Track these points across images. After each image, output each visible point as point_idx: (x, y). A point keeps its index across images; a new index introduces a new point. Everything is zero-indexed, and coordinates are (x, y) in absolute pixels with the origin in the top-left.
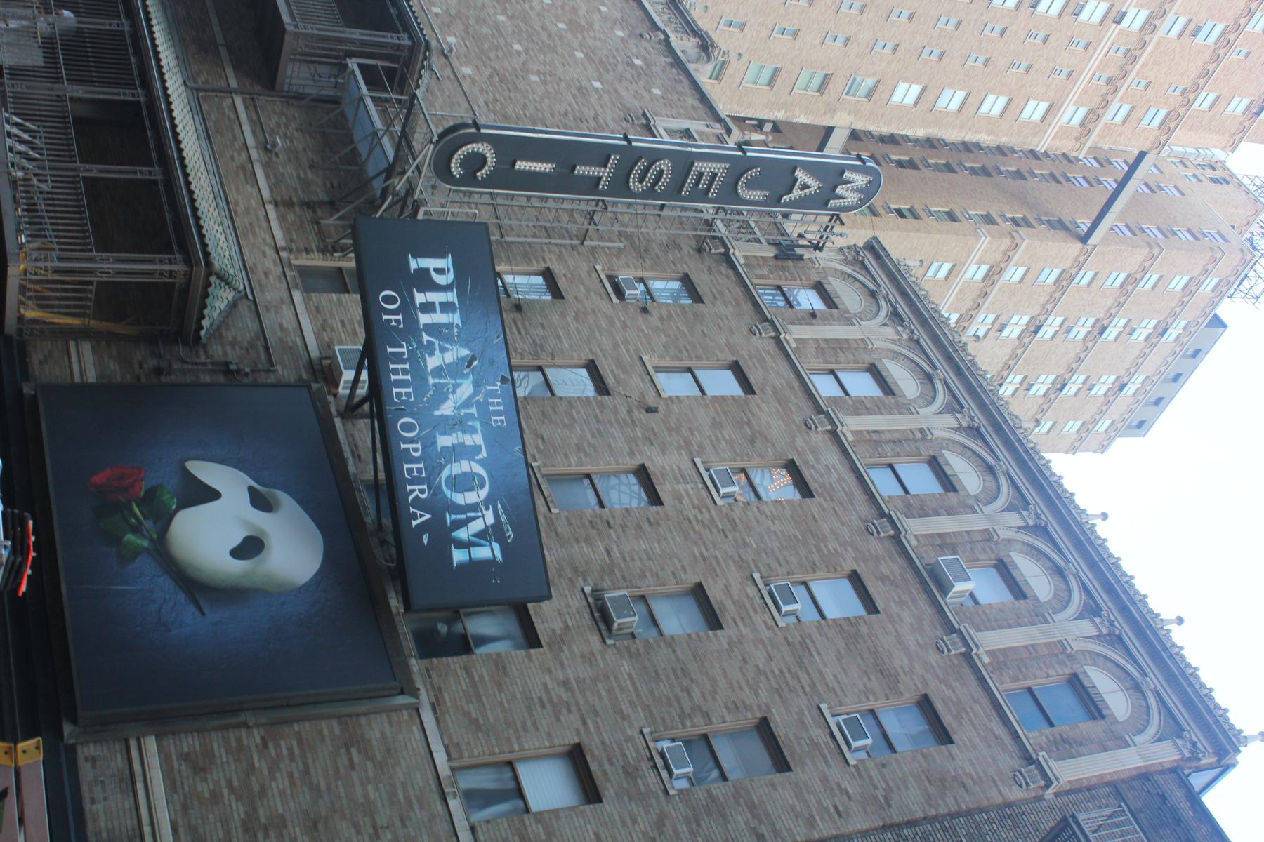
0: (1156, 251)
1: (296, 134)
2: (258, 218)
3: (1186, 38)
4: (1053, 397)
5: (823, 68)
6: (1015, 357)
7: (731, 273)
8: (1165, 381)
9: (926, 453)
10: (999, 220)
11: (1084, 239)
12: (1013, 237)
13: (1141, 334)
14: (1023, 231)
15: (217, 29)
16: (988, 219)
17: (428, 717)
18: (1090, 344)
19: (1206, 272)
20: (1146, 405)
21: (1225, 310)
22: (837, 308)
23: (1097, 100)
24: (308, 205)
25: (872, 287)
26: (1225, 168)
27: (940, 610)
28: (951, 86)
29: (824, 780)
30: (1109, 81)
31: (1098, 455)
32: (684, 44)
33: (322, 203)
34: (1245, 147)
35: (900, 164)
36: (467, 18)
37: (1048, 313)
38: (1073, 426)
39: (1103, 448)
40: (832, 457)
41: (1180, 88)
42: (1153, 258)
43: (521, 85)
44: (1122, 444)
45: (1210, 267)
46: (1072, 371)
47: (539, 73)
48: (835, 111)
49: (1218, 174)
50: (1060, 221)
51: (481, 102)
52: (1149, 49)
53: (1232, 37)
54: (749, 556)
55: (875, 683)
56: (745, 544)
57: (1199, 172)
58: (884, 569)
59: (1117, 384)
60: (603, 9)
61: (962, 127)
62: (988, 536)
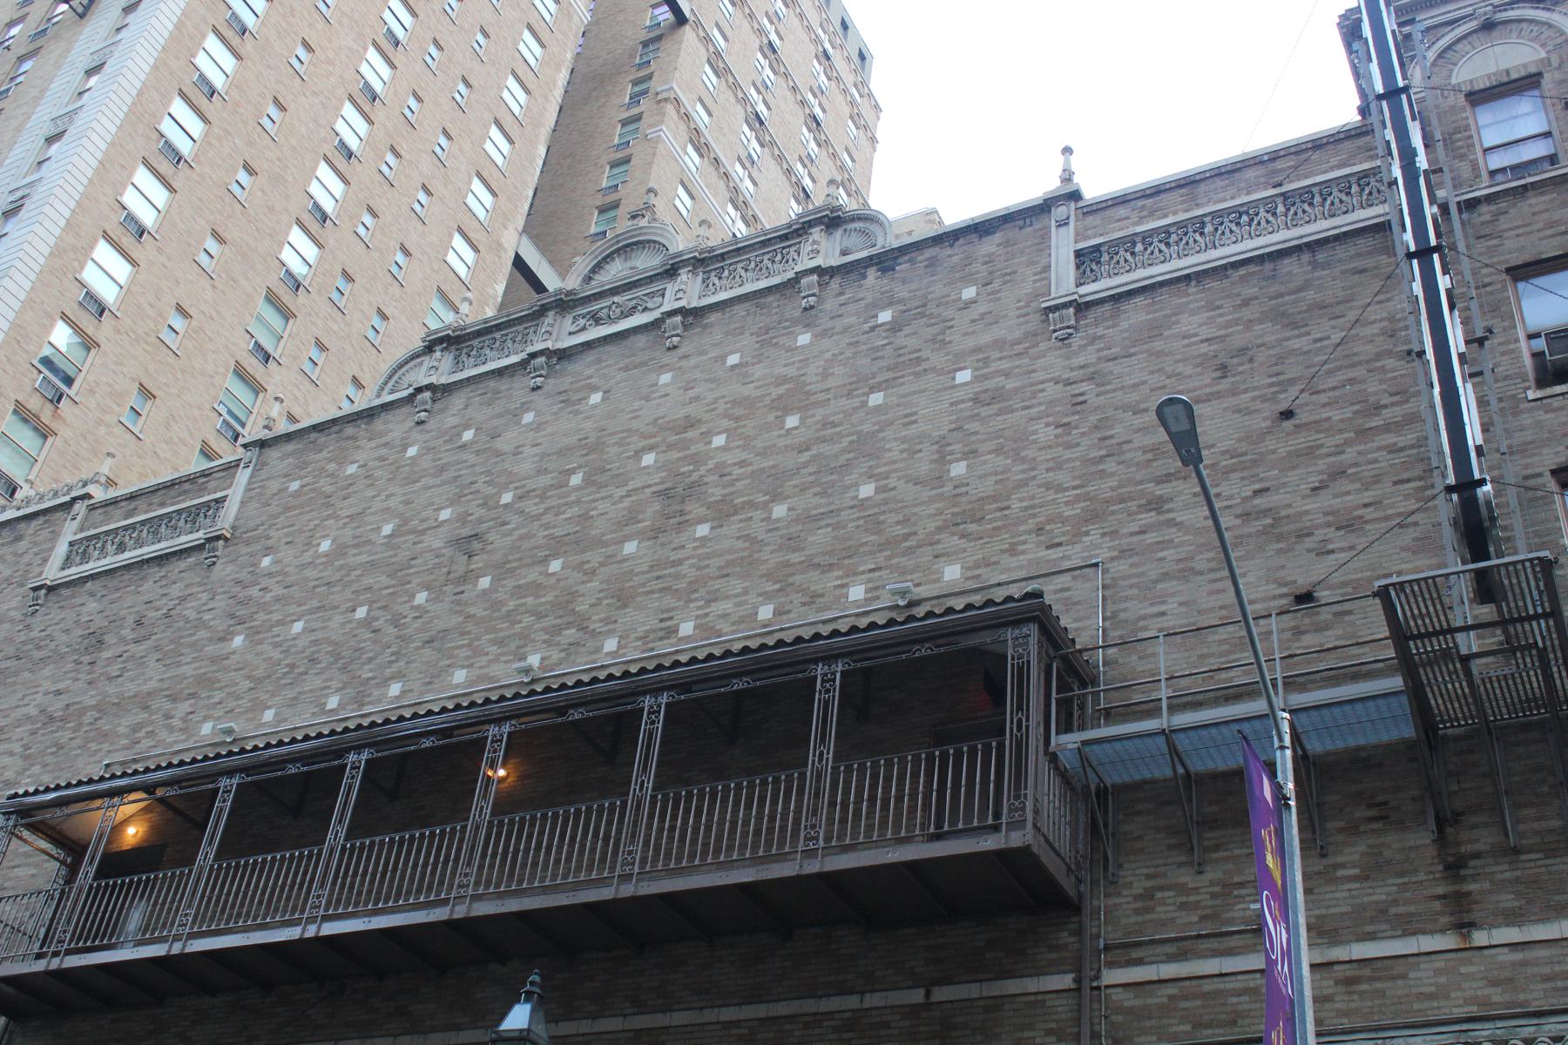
1: (1211, 874)
2: (1525, 963)
5: (451, 236)
6: (780, 158)
7: (1484, 208)
10: (635, 111)
11: (681, 19)
12: (666, 100)
14: (656, 85)
15: (873, 1000)
18: (782, 69)
22: (1540, 74)
24: (1455, 867)
25: (1473, 25)
28: (500, 89)
32: (826, 250)
33: (1441, 839)
36: (788, 564)
43: (988, 487)
44: (879, 82)
47: (943, 460)
48: (500, 244)
50: (645, 44)
51: (1043, 553)
59: (823, 60)
60: (733, 359)
61: (546, 99)
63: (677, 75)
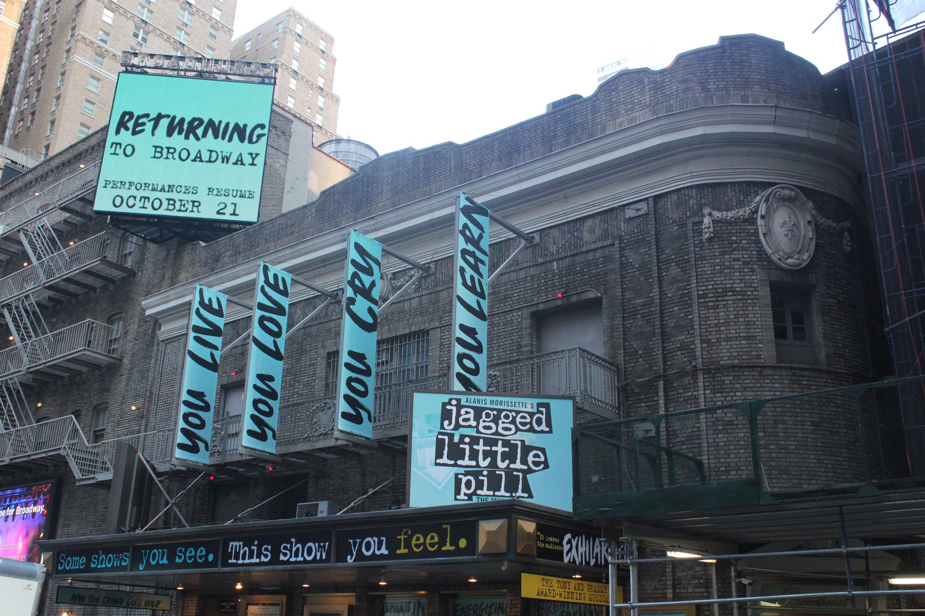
4: (194, 9)
16: (68, 51)
63: (83, 26)
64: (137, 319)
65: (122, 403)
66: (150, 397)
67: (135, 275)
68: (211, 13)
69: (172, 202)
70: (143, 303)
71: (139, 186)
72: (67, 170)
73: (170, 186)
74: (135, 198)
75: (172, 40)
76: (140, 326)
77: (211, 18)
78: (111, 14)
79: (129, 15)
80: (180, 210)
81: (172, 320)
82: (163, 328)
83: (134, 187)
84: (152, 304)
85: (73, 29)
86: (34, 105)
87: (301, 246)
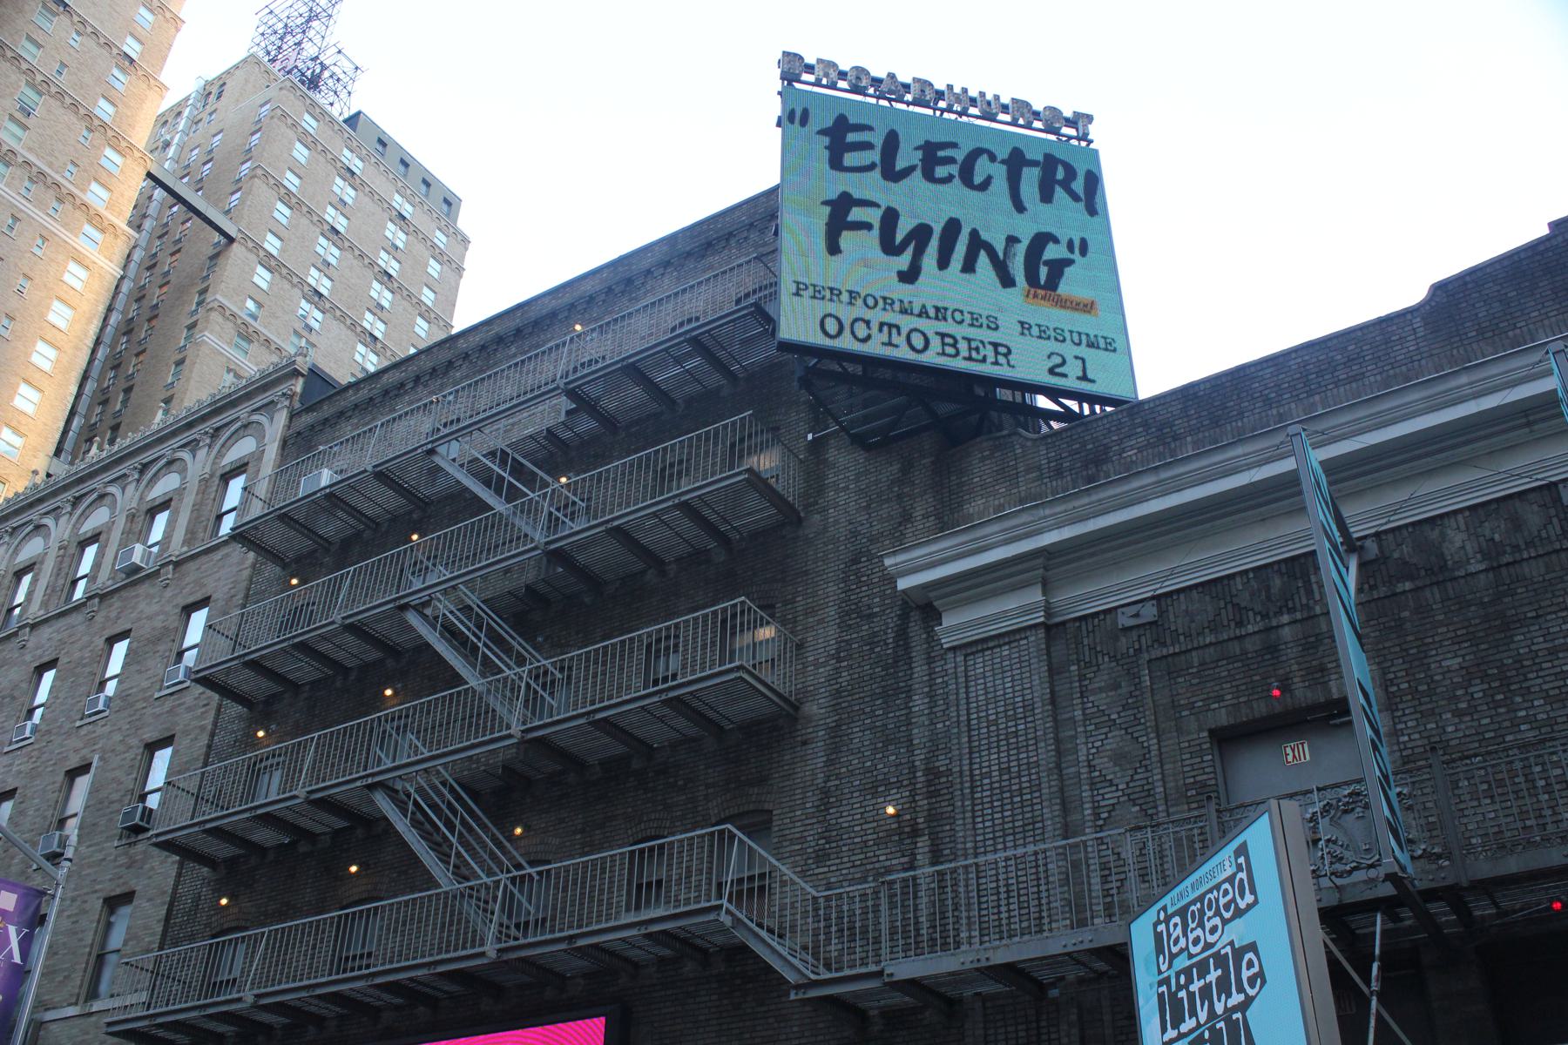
0: (259, 172)
3: (30, 122)
8: (405, 176)
9: (73, 550)
11: (231, 240)
13: (349, 194)
14: (209, 297)
16: (192, 327)
17: (50, 1016)
18: (347, 244)
19: (295, 125)
20: (427, 196)
21: (340, 111)
23: (78, 213)
26: (211, 83)
27: (148, 576)
29: (189, 709)
30: (60, 200)
31: (470, 246)
34: (164, 77)
35: (125, 402)
37: (303, 282)
38: (434, 268)
39: (465, 241)
40: (46, 632)
41: (85, 133)
42: (266, 175)
44: (464, 222)
45: (290, 121)
46: (372, 264)
49: (215, 90)
52: (32, 158)
53: (39, 78)
54: (68, 726)
55: (161, 648)
56: (60, 727)
57: (209, 109)
58: (113, 615)
62: (132, 518)
63: (223, 286)
64: (832, 611)
65: (825, 805)
66: (929, 783)
67: (800, 521)
68: (421, 293)
69: (948, 340)
70: (888, 562)
71: (871, 302)
72: (513, 350)
73: (937, 309)
74: (868, 323)
75: (359, 329)
76: (843, 626)
77: (420, 303)
78: (267, 275)
79: (295, 280)
80: (970, 359)
81: (995, 594)
82: (949, 620)
83: (859, 302)
84: (922, 562)
85: (204, 291)
86: (118, 414)
87: (1464, 379)
